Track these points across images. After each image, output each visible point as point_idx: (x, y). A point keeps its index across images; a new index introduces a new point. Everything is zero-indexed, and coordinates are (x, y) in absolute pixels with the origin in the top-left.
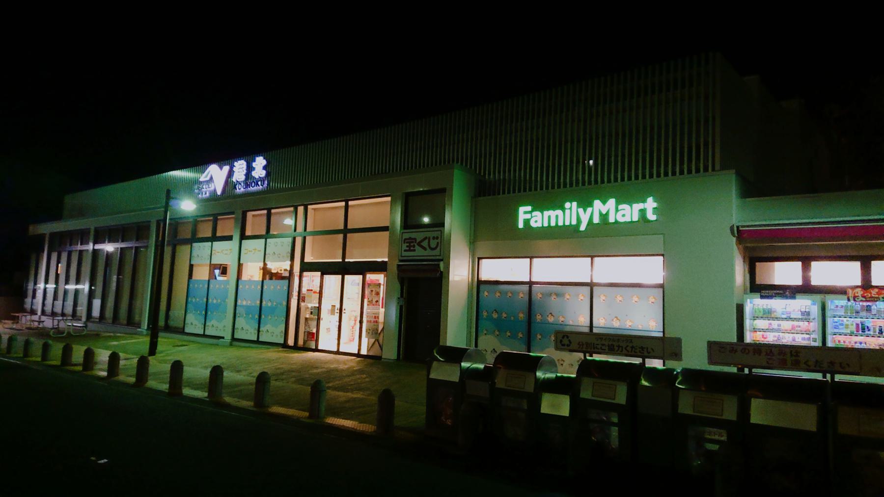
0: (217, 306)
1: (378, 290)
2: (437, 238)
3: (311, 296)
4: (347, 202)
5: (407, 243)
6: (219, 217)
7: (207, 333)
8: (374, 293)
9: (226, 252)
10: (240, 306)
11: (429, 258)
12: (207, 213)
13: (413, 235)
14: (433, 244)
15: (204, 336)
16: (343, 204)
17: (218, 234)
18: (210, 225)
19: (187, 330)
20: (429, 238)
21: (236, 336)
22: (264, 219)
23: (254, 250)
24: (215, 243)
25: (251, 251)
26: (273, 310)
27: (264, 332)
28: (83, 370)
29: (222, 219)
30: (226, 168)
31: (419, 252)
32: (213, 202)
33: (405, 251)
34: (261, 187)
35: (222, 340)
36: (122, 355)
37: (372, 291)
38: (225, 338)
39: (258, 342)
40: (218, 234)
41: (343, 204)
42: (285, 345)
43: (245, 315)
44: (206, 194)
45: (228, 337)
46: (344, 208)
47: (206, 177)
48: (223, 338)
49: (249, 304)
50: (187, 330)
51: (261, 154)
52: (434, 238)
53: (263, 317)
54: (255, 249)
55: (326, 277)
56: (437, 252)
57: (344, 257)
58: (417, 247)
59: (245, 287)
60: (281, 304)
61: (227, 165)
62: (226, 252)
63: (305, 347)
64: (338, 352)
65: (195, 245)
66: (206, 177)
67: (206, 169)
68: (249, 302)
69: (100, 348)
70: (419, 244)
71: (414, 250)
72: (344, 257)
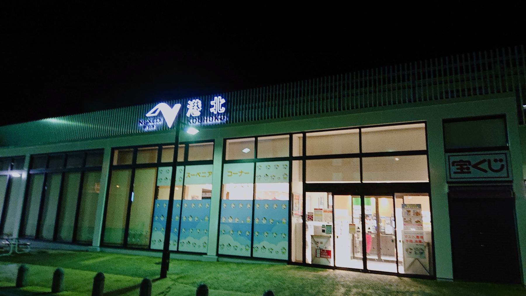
0: (194, 225)
1: (418, 211)
2: (501, 160)
3: (321, 215)
4: (256, 137)
5: (457, 165)
6: (139, 149)
7: (180, 249)
8: (412, 213)
9: (204, 175)
10: (224, 223)
11: (462, 180)
12: (204, 139)
13: (465, 158)
14: (496, 166)
15: (252, 258)
16: (254, 139)
17: (190, 159)
18: (172, 152)
19: (153, 247)
20: (489, 161)
21: (220, 253)
22: (253, 145)
23: (240, 172)
24: (187, 167)
25: (237, 174)
26: (269, 228)
27: (157, 241)
28: (52, 291)
29: (193, 146)
30: (178, 107)
31: (475, 174)
32: (210, 129)
33: (455, 173)
34: (220, 121)
35: (204, 256)
36: (106, 275)
37: (409, 211)
38: (208, 254)
39: (252, 258)
40: (190, 159)
41: (357, 130)
42: (289, 262)
43: (232, 232)
44: (153, 126)
45: (212, 253)
46: (254, 142)
47: (154, 112)
48: (206, 254)
49: (236, 222)
50: (153, 247)
51: (198, 98)
52: (496, 161)
53: (256, 233)
54: (242, 172)
55: (335, 196)
56: (504, 173)
57: (361, 180)
58: (472, 169)
59: (198, 205)
60: (280, 222)
61: (178, 103)
62: (204, 175)
63: (314, 263)
64: (365, 270)
65: (160, 169)
66: (154, 112)
67: (155, 106)
68: (237, 220)
69: (67, 267)
70: (475, 166)
71: (470, 173)
72: (361, 180)
